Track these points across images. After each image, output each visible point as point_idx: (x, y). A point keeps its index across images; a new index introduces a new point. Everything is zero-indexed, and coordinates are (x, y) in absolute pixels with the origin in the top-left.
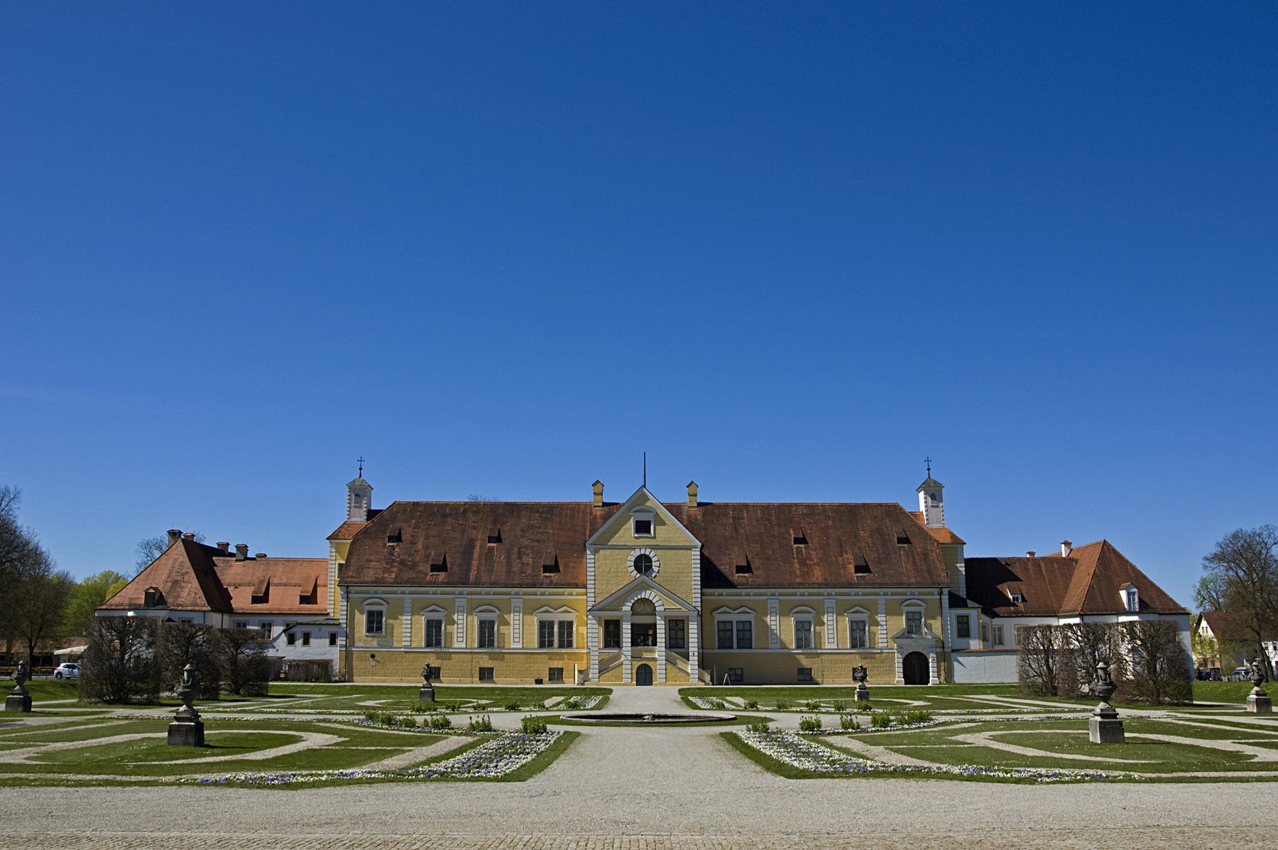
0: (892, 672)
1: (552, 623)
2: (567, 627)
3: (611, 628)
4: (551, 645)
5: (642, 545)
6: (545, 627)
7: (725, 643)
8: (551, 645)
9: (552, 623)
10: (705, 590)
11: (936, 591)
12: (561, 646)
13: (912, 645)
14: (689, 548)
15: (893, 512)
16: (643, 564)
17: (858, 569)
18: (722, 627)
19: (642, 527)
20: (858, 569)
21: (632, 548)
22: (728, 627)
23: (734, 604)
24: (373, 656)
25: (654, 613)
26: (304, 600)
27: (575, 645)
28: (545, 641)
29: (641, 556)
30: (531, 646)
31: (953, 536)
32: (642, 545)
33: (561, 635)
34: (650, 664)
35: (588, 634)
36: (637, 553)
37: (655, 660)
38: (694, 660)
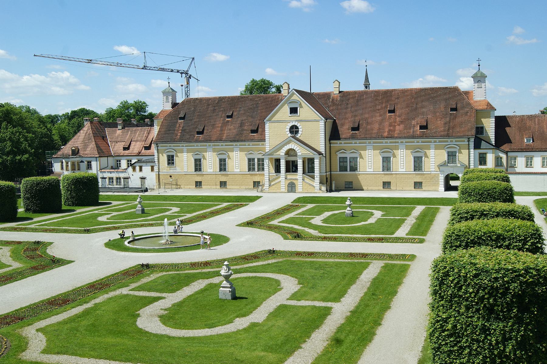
0: (438, 184)
1: (254, 159)
5: (293, 120)
7: (343, 169)
8: (254, 169)
10: (332, 141)
11: (466, 140)
12: (258, 170)
13: (449, 170)
14: (318, 121)
15: (452, 93)
16: (294, 130)
17: (422, 127)
18: (341, 160)
19: (294, 111)
20: (422, 127)
21: (289, 122)
23: (346, 148)
24: (171, 176)
25: (296, 156)
28: (251, 168)
31: (489, 104)
32: (293, 120)
33: (259, 165)
34: (294, 181)
36: (290, 125)
37: (297, 179)
38: (317, 179)
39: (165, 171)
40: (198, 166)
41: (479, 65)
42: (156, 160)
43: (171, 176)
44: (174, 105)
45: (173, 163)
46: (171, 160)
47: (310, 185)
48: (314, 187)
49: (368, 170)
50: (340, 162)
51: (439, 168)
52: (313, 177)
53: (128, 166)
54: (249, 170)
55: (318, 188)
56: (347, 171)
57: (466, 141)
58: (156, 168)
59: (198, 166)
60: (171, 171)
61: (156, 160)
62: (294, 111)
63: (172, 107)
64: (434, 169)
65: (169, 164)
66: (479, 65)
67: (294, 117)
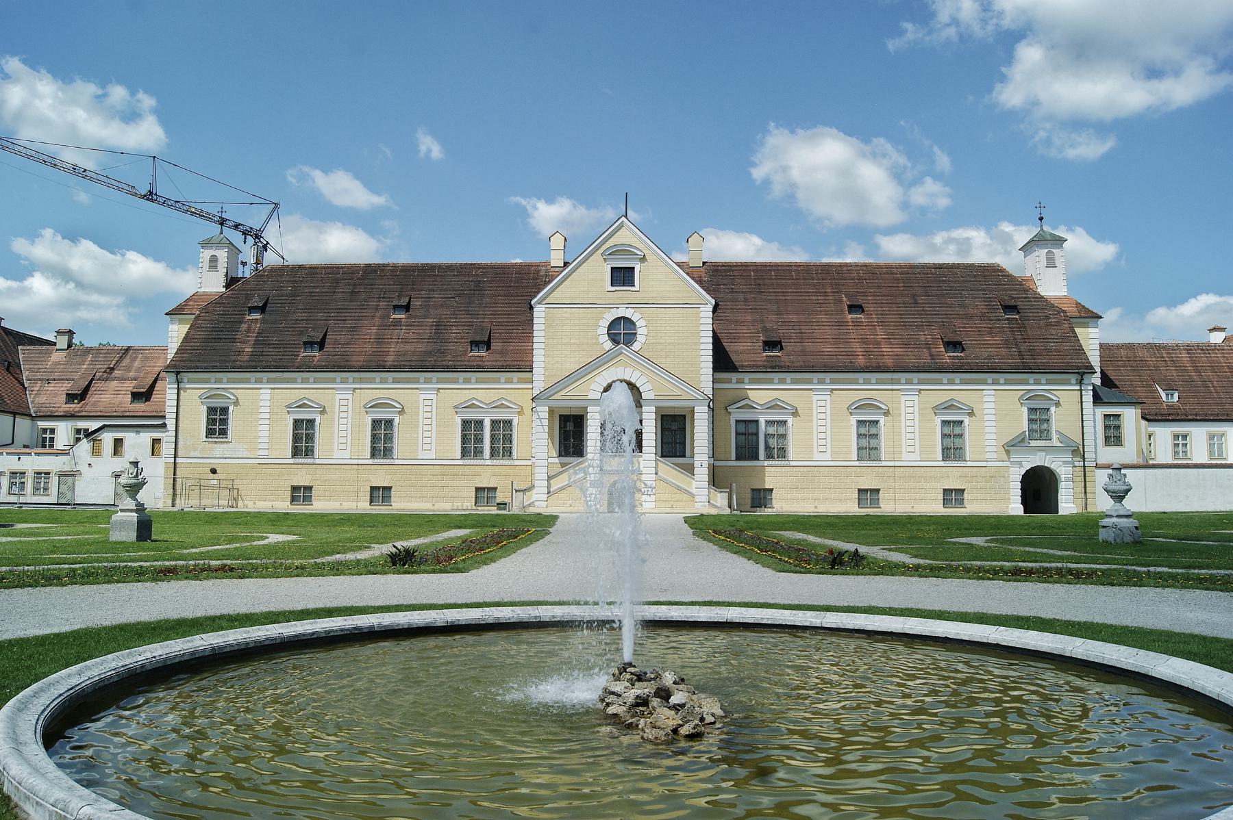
1: (479, 423)
2: (503, 429)
3: (570, 427)
4: (478, 453)
5: (621, 303)
6: (471, 430)
8: (478, 453)
9: (479, 423)
15: (989, 275)
16: (621, 331)
18: (742, 430)
19: (623, 276)
22: (752, 429)
24: (214, 471)
26: (136, 396)
27: (515, 455)
29: (618, 319)
30: (450, 455)
32: (621, 303)
35: (535, 438)
38: (702, 473)
39: (197, 454)
40: (303, 439)
41: (1041, 219)
42: (171, 422)
43: (214, 471)
44: (231, 282)
45: (224, 433)
46: (217, 423)
47: (679, 488)
48: (693, 496)
49: (817, 456)
50: (737, 434)
51: (1008, 452)
52: (690, 469)
53: (78, 440)
54: (465, 453)
55: (705, 498)
56: (756, 458)
57: (1073, 381)
58: (167, 448)
59: (303, 439)
60: (219, 451)
61: (171, 422)
62: (623, 276)
63: (227, 286)
64: (994, 455)
65: (210, 433)
66: (1041, 219)
67: (623, 292)
